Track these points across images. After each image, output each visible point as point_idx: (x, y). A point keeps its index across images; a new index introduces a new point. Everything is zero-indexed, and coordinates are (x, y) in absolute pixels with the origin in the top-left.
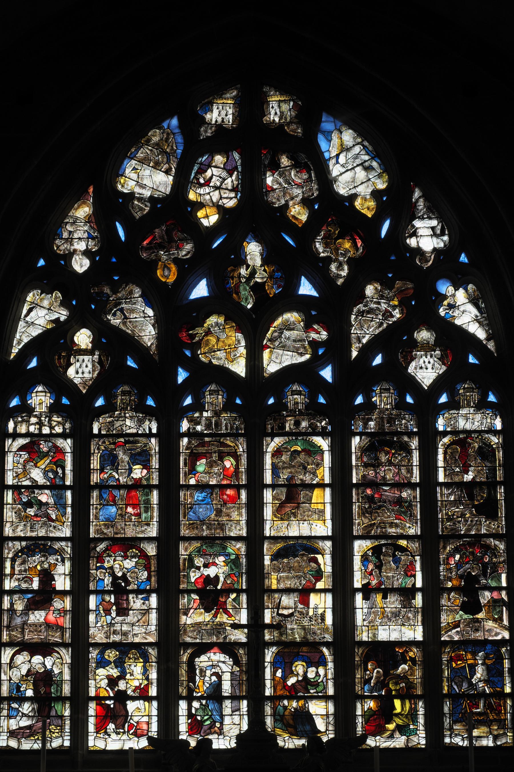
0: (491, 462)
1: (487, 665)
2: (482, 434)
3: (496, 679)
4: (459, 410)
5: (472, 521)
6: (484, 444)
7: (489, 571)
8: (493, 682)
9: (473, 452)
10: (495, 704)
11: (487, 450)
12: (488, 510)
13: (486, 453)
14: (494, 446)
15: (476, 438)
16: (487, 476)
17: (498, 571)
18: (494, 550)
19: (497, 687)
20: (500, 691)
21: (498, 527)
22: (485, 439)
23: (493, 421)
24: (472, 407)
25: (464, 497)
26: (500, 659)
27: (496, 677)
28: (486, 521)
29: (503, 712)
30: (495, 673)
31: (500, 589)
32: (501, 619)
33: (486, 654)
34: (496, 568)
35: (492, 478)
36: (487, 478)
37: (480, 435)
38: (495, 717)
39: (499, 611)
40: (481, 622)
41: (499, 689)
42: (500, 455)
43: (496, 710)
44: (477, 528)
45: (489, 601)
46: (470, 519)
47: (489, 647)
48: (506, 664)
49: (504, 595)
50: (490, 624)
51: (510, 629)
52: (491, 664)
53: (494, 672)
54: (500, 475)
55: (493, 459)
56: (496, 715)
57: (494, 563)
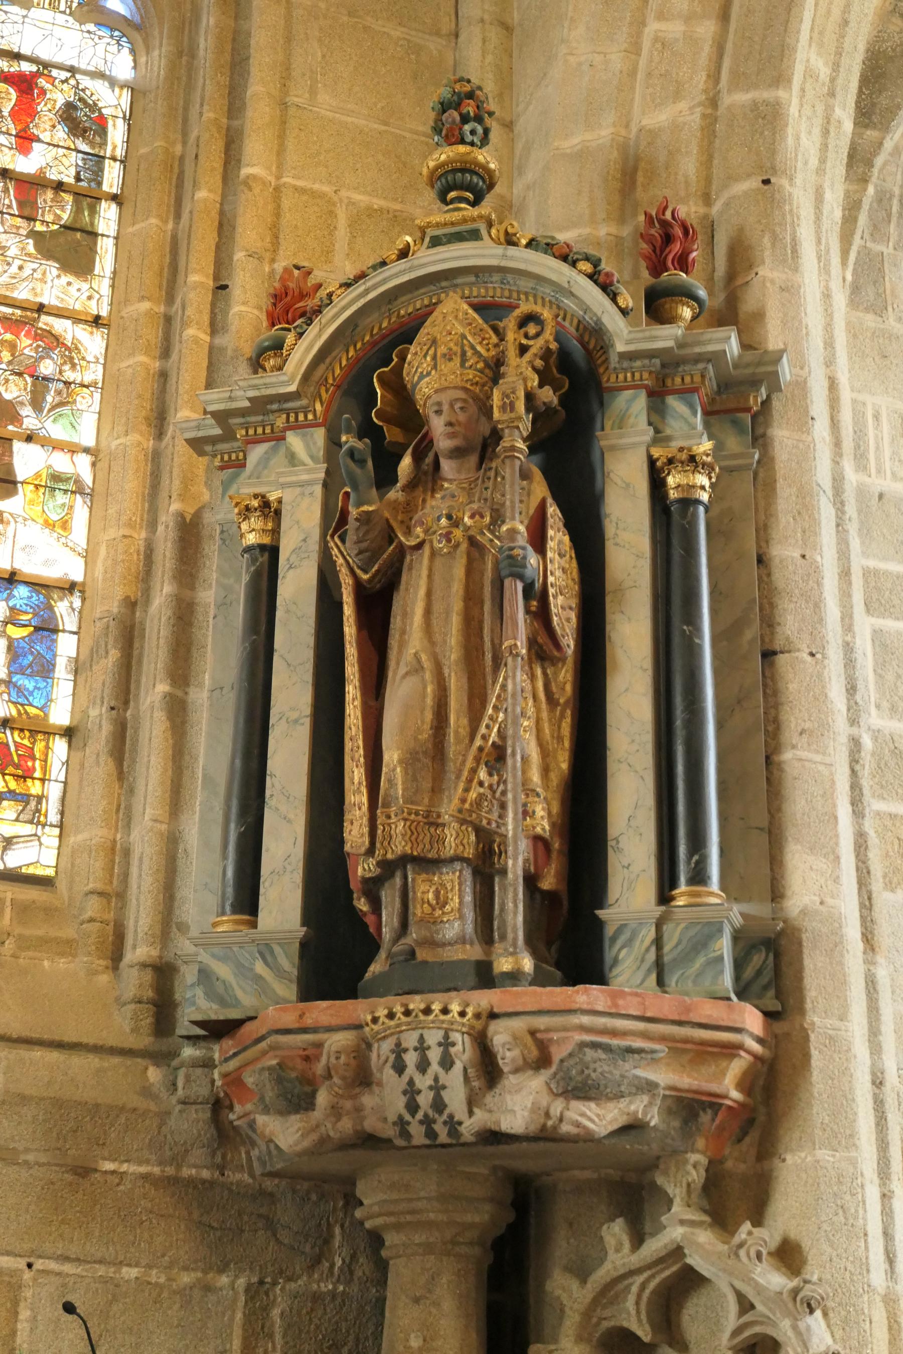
0: (92, 144)
1: (9, 639)
2: (78, 76)
3: (29, 684)
4: (29, 9)
5: (21, 268)
6: (81, 99)
7: (49, 399)
8: (20, 690)
9: (50, 111)
10: (17, 750)
11: (86, 115)
12: (71, 249)
13: (82, 121)
14: (104, 111)
15: (63, 82)
16: (78, 173)
17: (75, 402)
18: (68, 348)
19: (31, 705)
20: (37, 716)
21: (90, 298)
22: (83, 90)
23: (109, 57)
24: (64, 12)
25: (10, 207)
26: (47, 628)
27: (30, 676)
28: (59, 276)
29: (38, 774)
30: (30, 666)
31: (73, 449)
32: (65, 525)
33: (12, 609)
34: (69, 395)
35: (90, 181)
36: (78, 178)
37: (73, 76)
38: (13, 785)
39: (63, 505)
40: (8, 523)
41: (32, 711)
42: (117, 134)
43: (17, 766)
44: (33, 289)
45: (38, 475)
46: (18, 263)
47: (22, 591)
48: (66, 646)
49: (83, 466)
50: (32, 534)
51: (89, 556)
52: (23, 638)
53: (26, 662)
54: (112, 178)
55: (98, 139)
56: (16, 777)
57: (67, 384)
